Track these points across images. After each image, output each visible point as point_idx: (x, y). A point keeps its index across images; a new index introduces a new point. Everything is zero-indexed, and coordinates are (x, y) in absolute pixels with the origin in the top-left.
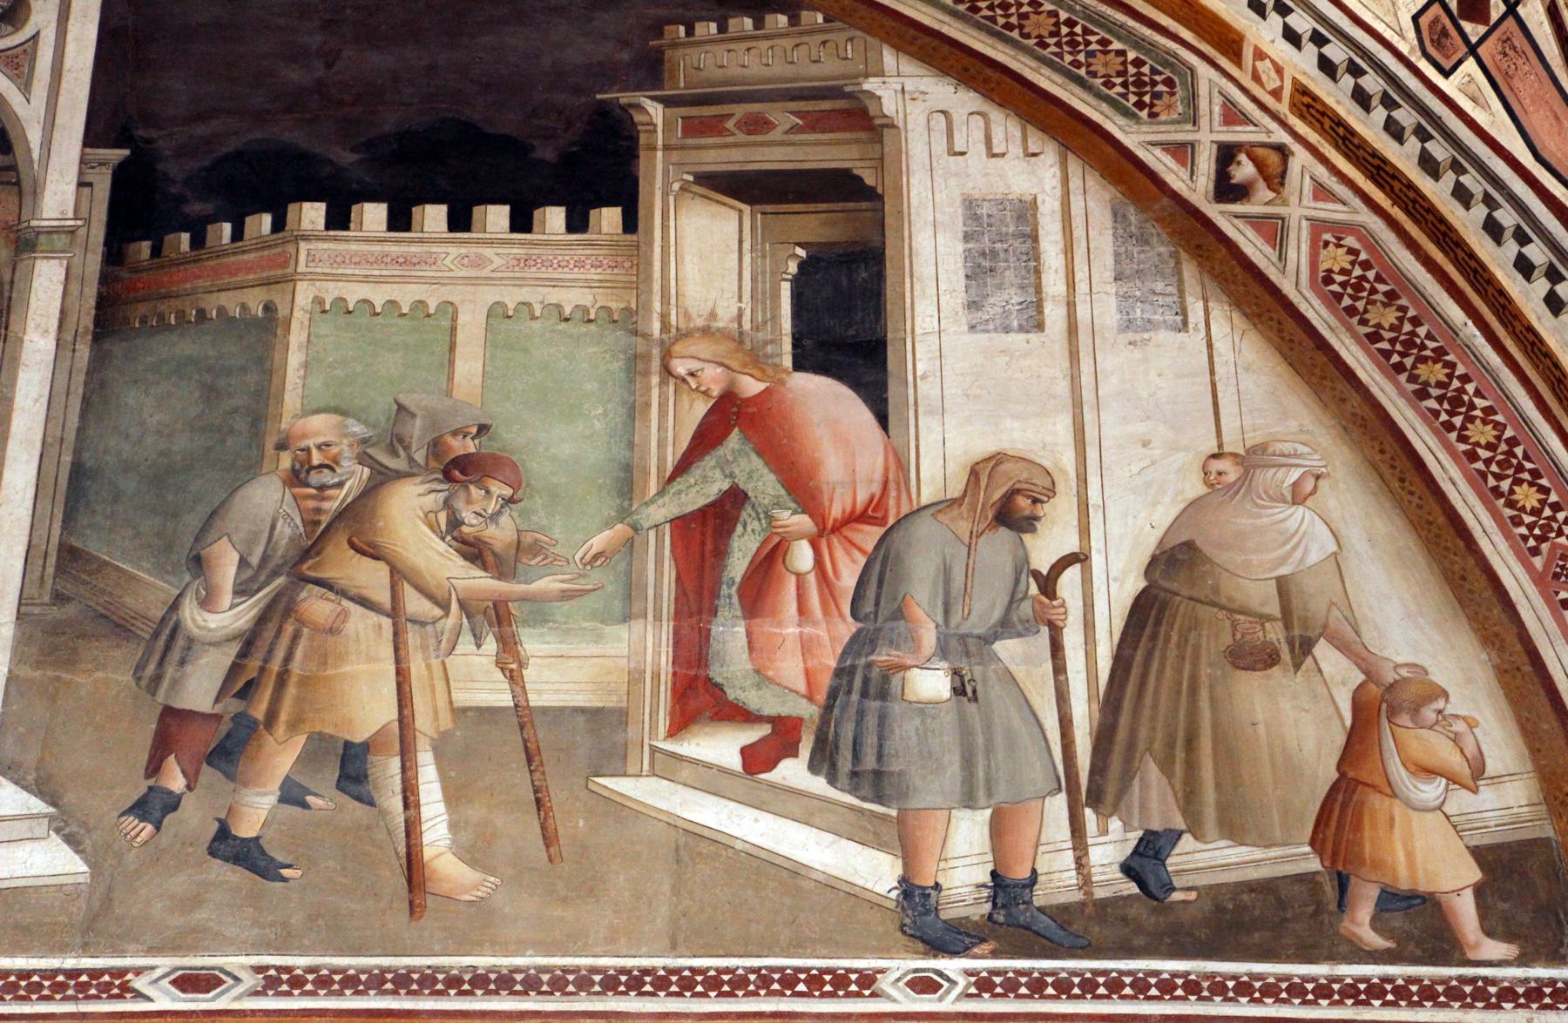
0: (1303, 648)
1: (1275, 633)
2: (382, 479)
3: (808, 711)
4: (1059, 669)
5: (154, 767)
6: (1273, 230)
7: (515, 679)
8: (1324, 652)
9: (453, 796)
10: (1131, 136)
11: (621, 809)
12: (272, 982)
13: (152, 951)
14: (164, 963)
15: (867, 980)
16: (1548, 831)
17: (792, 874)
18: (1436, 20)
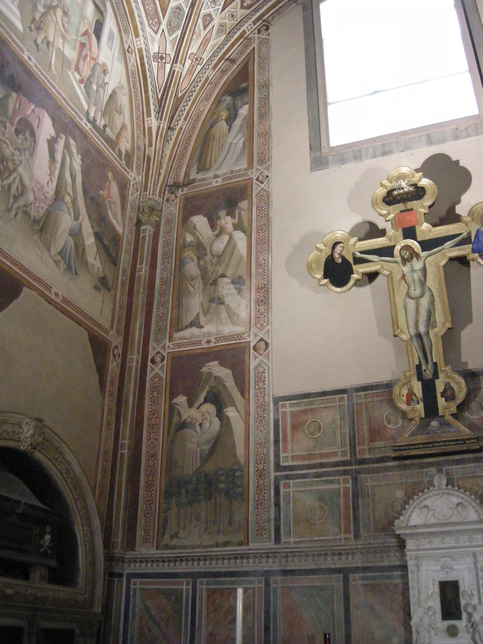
0: (120, 114)
1: (119, 109)
2: (57, 6)
3: (85, 80)
4: (104, 96)
5: (31, 24)
6: (130, 60)
7: (64, 47)
8: (121, 115)
9: (56, 58)
10: (123, 36)
11: (68, 75)
12: (36, 66)
13: (27, 49)
14: (27, 53)
15: (82, 119)
16: (130, 152)
17: (79, 100)
18: (156, 55)
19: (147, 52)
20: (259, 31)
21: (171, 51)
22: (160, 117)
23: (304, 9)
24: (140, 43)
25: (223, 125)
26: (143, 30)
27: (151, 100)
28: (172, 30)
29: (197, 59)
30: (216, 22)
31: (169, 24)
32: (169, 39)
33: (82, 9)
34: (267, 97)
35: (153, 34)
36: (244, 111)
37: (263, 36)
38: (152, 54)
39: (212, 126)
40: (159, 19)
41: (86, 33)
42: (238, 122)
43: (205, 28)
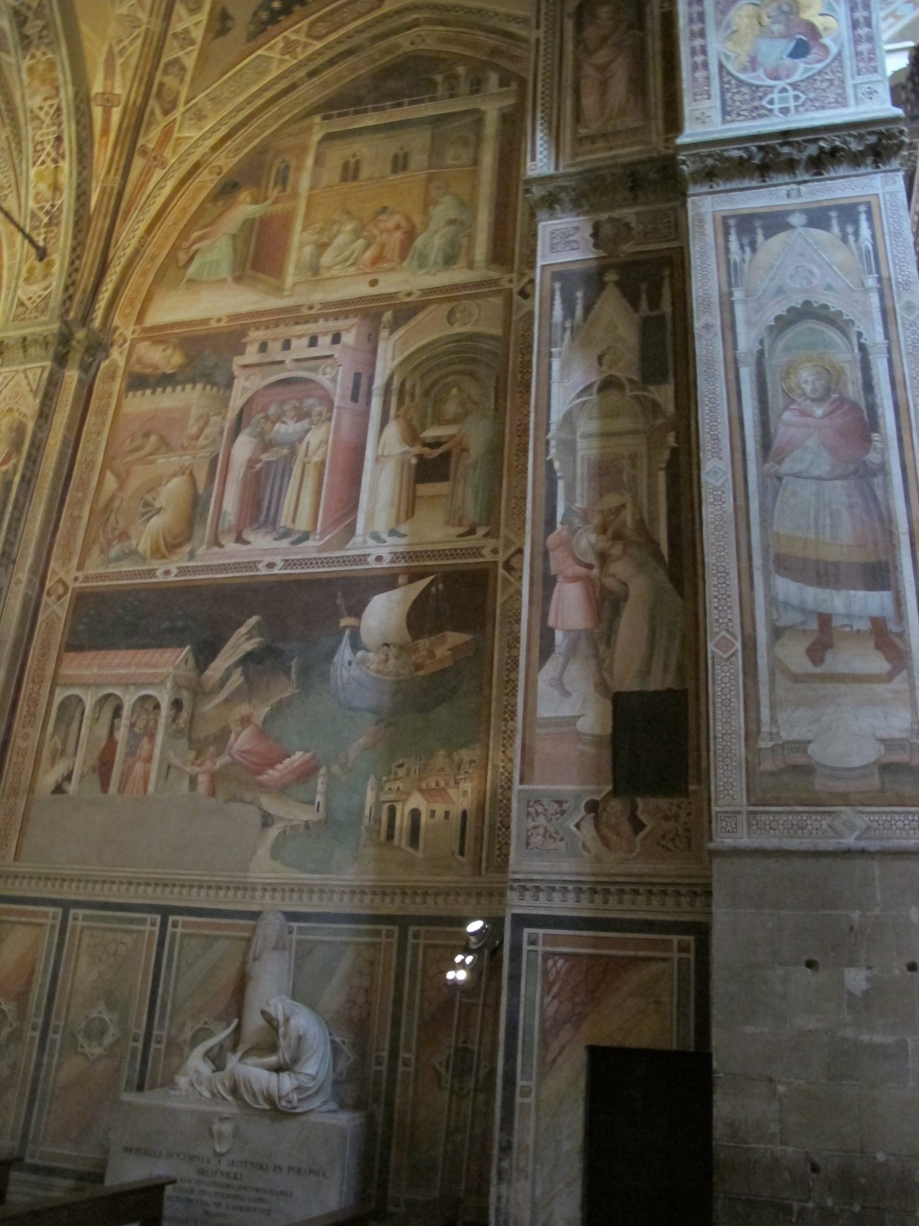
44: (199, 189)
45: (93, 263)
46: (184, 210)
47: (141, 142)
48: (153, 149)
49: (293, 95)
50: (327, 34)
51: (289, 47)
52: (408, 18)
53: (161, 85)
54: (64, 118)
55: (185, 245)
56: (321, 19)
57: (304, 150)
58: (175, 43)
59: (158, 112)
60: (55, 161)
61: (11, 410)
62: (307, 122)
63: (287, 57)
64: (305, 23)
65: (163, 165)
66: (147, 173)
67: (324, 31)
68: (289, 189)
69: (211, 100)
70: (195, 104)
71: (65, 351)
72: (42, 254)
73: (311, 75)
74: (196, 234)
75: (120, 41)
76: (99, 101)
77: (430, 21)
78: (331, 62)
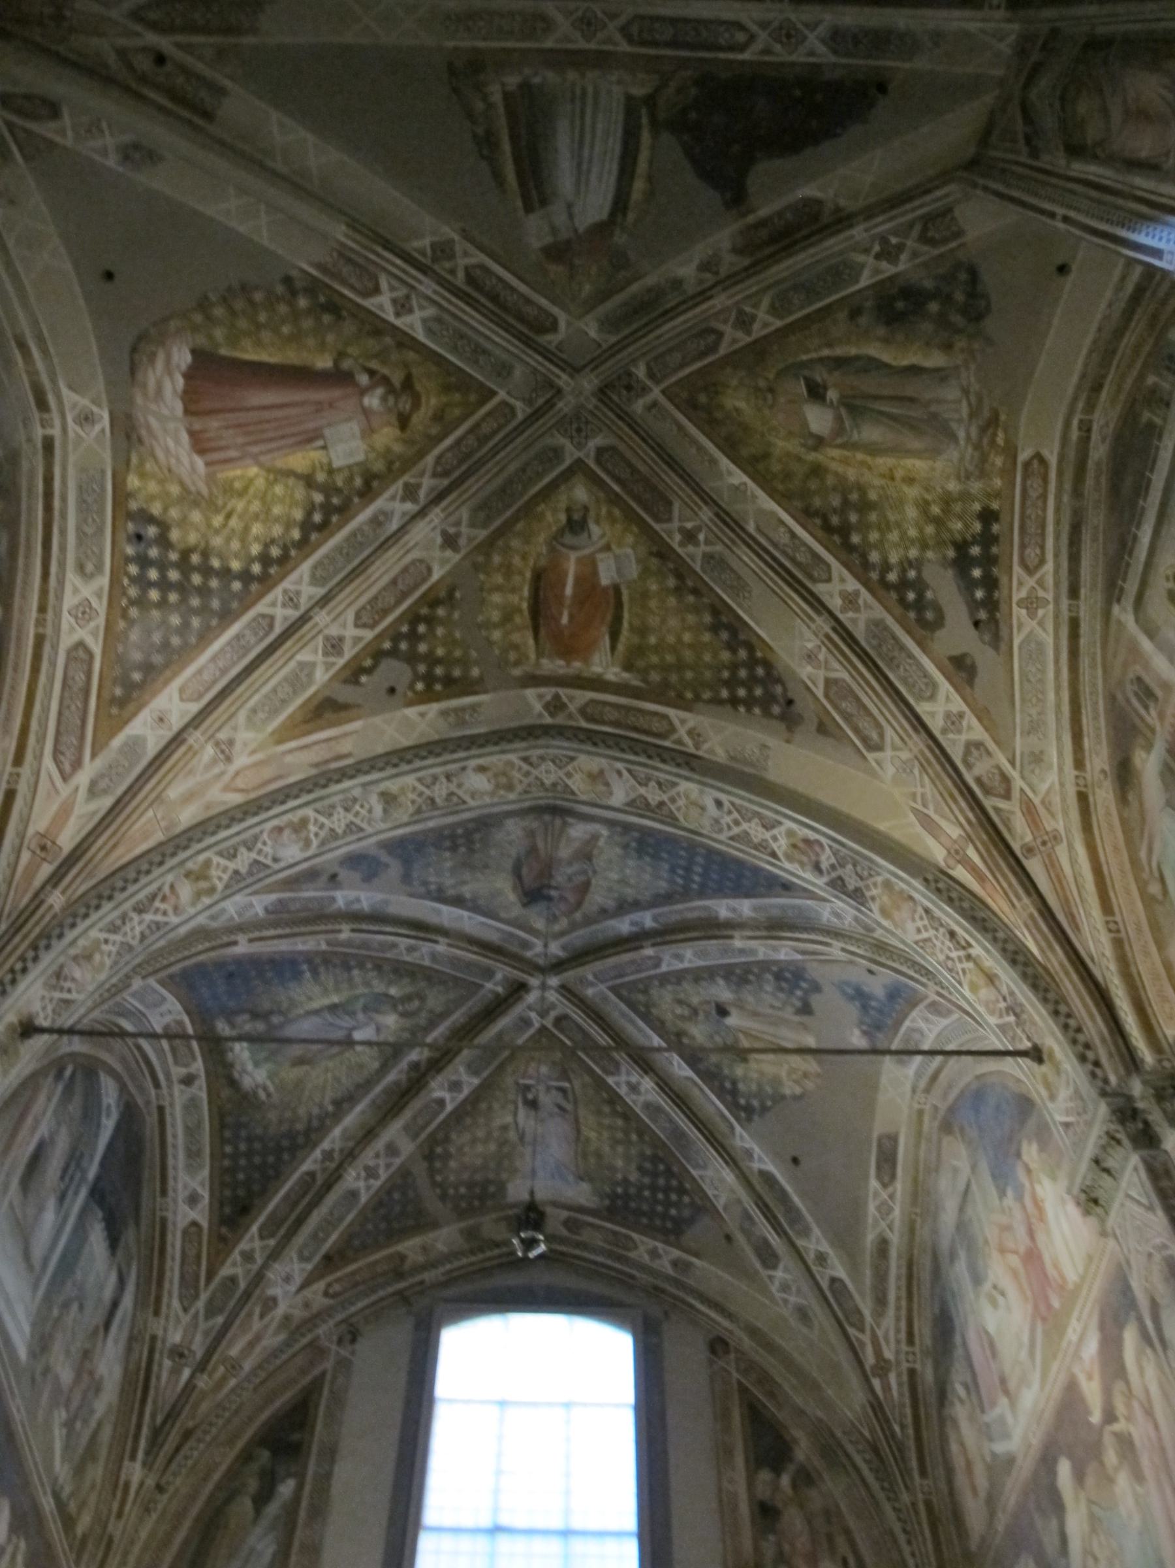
19: (164, 1341)
20: (340, 1341)
21: (198, 1347)
22: (147, 1465)
23: (417, 1327)
24: (156, 1327)
25: (245, 1505)
26: (169, 1306)
27: (145, 1431)
28: (211, 1312)
29: (234, 1366)
30: (281, 1310)
31: (210, 1302)
32: (203, 1325)
33: (101, 1288)
34: (328, 1476)
35: (181, 1313)
36: (286, 1489)
37: (344, 1353)
38: (168, 1345)
39: (228, 1500)
40: (196, 1288)
41: (95, 1332)
42: (273, 1509)
43: (262, 1316)
44: (1108, 814)
45: (1085, 1005)
46: (1116, 849)
47: (1016, 847)
48: (1035, 839)
49: (1084, 628)
50: (1042, 547)
51: (1031, 604)
52: (1075, 434)
53: (979, 780)
54: (937, 913)
55: (1145, 876)
56: (1023, 546)
57: (1134, 650)
58: (951, 736)
59: (1002, 804)
60: (969, 957)
61: (1150, 1255)
62: (1113, 627)
63: (1041, 612)
64: (1017, 569)
65: (1056, 838)
66: (1051, 865)
67: (1038, 551)
68: (1159, 693)
69: (1029, 733)
70: (1022, 754)
71: (1140, 1126)
72: (1036, 1054)
73: (1074, 593)
74: (1143, 854)
75: (914, 795)
76: (951, 862)
77: (1090, 407)
78: (1075, 558)
